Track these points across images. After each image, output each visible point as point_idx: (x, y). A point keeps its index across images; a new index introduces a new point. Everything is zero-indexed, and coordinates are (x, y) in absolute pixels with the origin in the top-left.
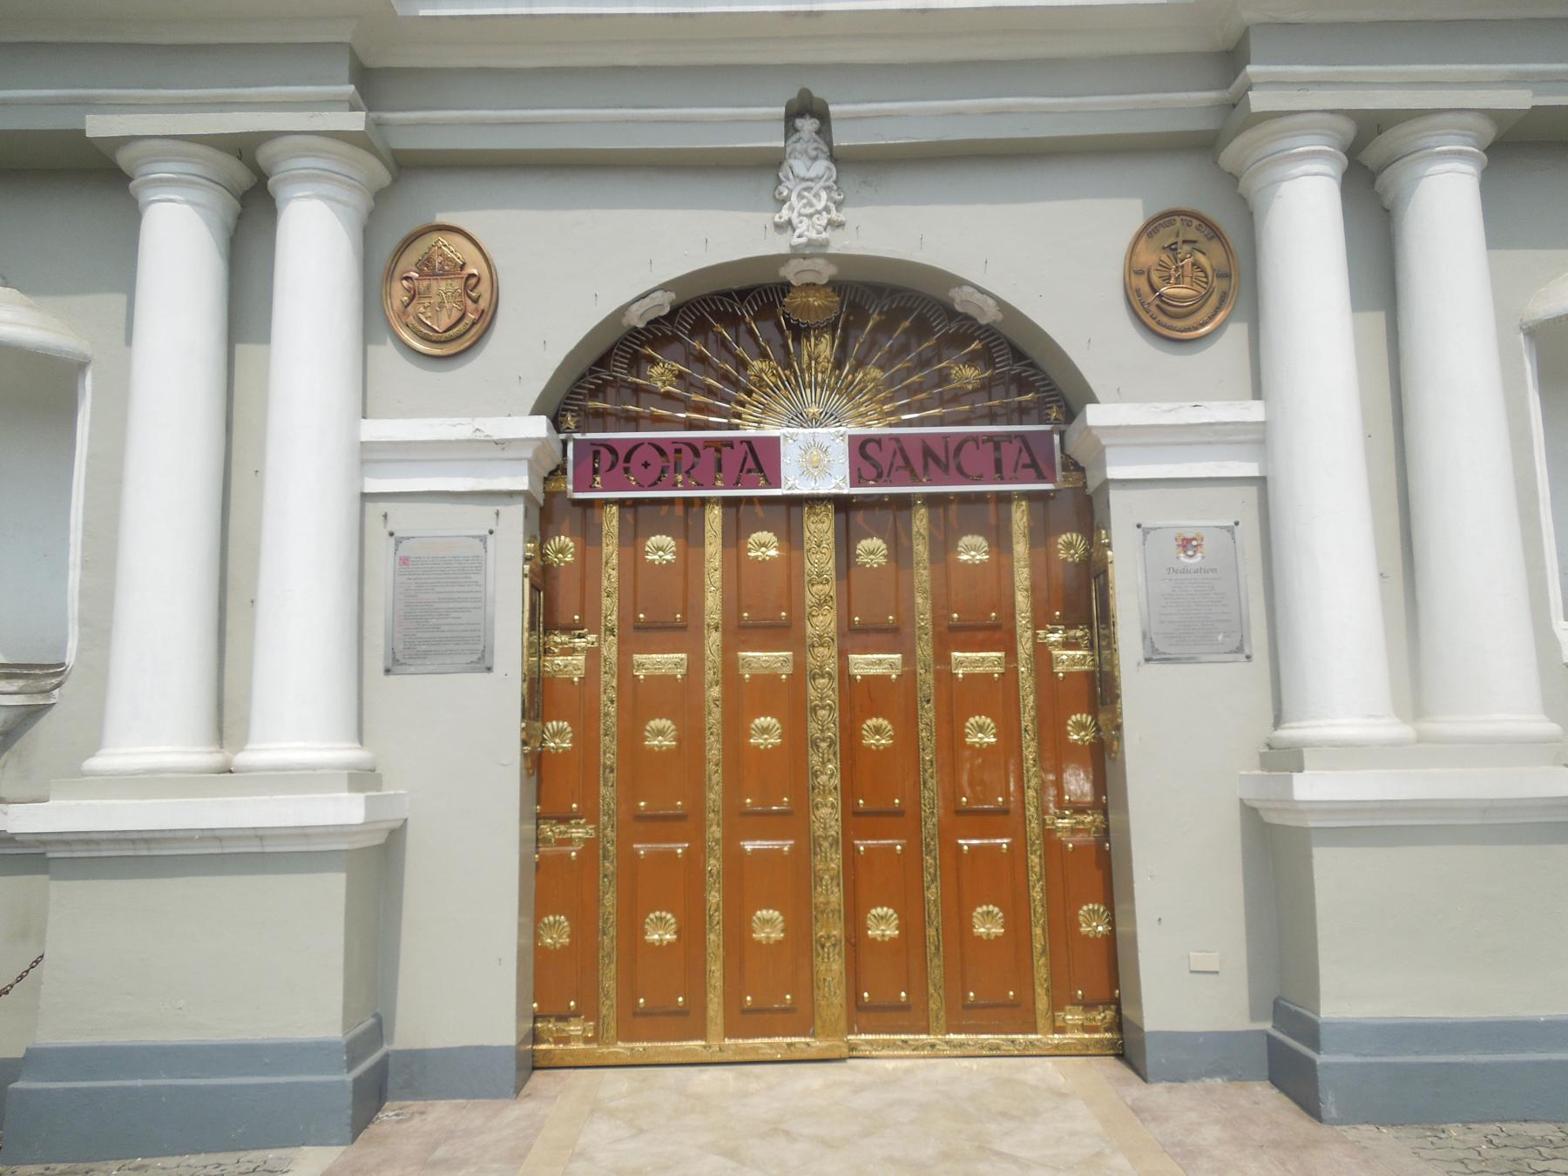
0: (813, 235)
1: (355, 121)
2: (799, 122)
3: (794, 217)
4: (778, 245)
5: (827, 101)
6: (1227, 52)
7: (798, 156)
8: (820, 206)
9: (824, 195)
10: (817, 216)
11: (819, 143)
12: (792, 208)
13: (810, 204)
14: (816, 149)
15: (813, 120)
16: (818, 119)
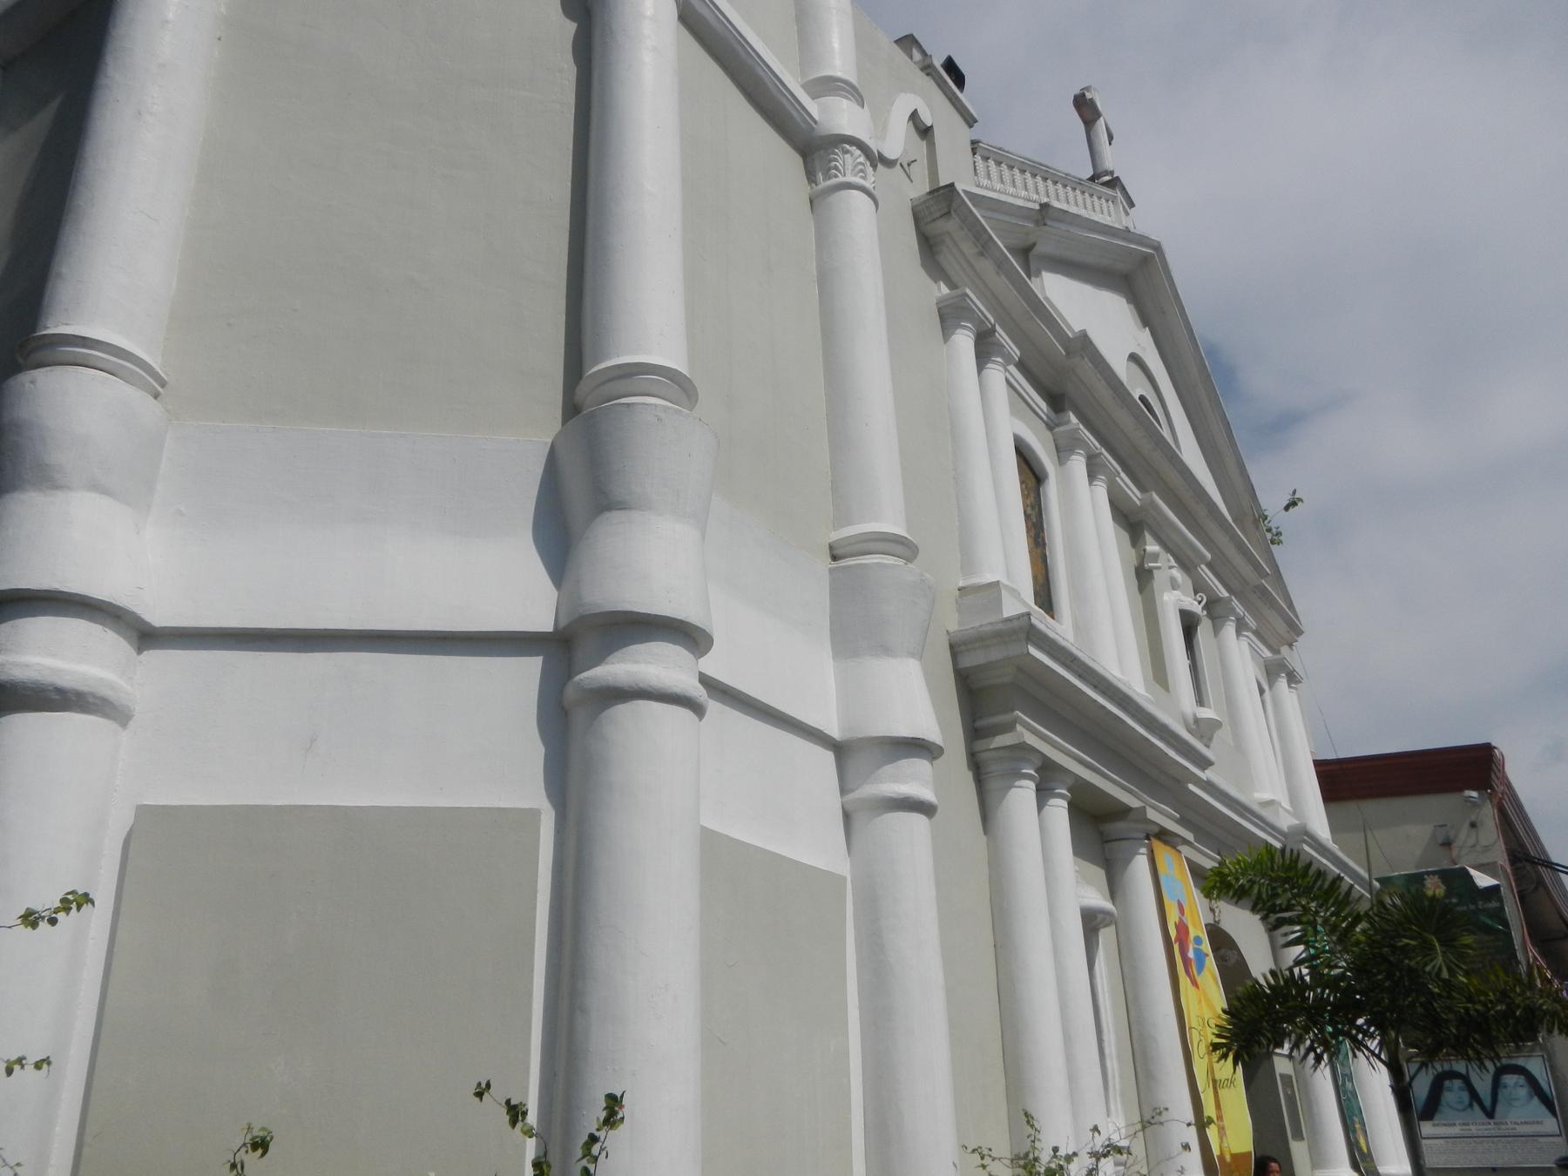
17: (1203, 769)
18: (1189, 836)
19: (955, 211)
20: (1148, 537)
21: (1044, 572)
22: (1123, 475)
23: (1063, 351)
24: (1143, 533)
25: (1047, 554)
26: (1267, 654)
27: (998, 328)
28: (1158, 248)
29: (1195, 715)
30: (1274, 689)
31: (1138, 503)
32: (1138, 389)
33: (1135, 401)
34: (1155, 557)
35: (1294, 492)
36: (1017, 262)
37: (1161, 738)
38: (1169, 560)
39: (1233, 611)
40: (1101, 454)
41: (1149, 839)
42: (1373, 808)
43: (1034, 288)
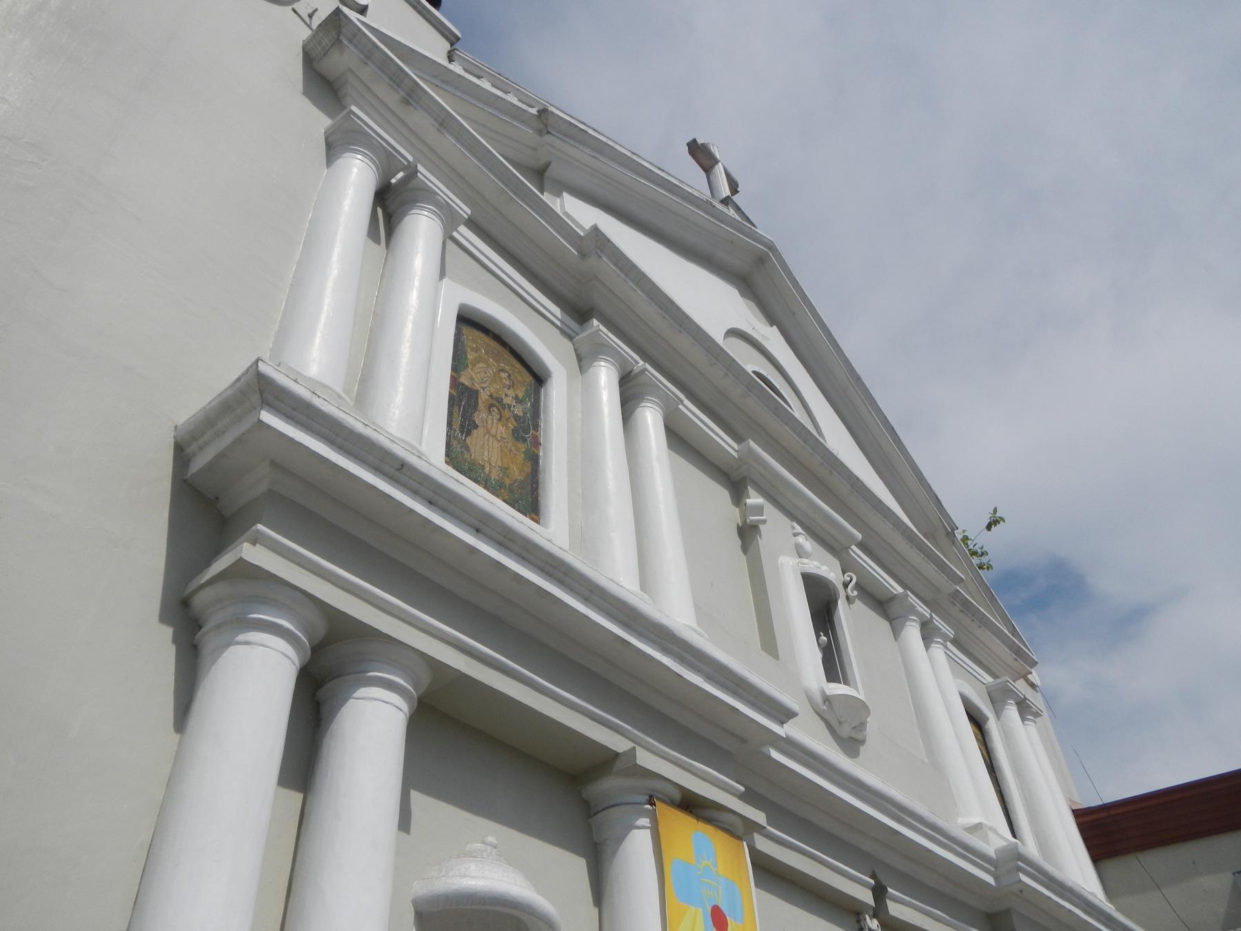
17: (782, 723)
18: (759, 817)
19: (350, 41)
20: (751, 491)
21: (528, 469)
22: (687, 402)
23: (575, 252)
24: (746, 488)
25: (541, 454)
26: (988, 679)
27: (420, 168)
28: (772, 247)
29: (823, 692)
30: (1002, 719)
31: (735, 454)
32: (751, 363)
33: (748, 373)
34: (759, 510)
35: (995, 510)
36: (533, 185)
37: (666, 651)
38: (793, 528)
39: (912, 609)
40: (646, 369)
41: (652, 804)
42: (1157, 860)
43: (546, 200)
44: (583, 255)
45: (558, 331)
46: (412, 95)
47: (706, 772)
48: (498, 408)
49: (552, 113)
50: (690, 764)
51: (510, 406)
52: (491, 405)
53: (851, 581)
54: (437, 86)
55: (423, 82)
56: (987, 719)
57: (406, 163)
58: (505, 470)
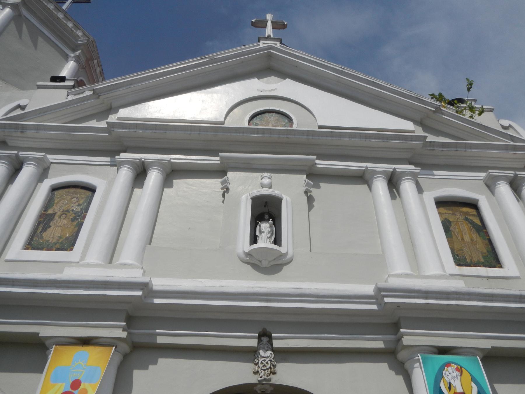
0: (266, 377)
1: (124, 335)
2: (263, 338)
3: (259, 370)
4: (253, 379)
5: (271, 332)
6: (395, 323)
7: (262, 349)
8: (268, 367)
9: (269, 362)
10: (267, 370)
11: (269, 345)
12: (259, 367)
13: (264, 366)
14: (267, 347)
15: (267, 338)
16: (268, 337)
21: (76, 229)
30: (496, 194)
44: (110, 132)
45: (109, 166)
46: (23, 128)
47: (98, 324)
48: (66, 214)
49: (96, 89)
50: (88, 324)
51: (73, 210)
52: (63, 214)
53: (306, 181)
54: (41, 116)
55: (25, 122)
56: (477, 201)
57: (14, 155)
58: (60, 237)
